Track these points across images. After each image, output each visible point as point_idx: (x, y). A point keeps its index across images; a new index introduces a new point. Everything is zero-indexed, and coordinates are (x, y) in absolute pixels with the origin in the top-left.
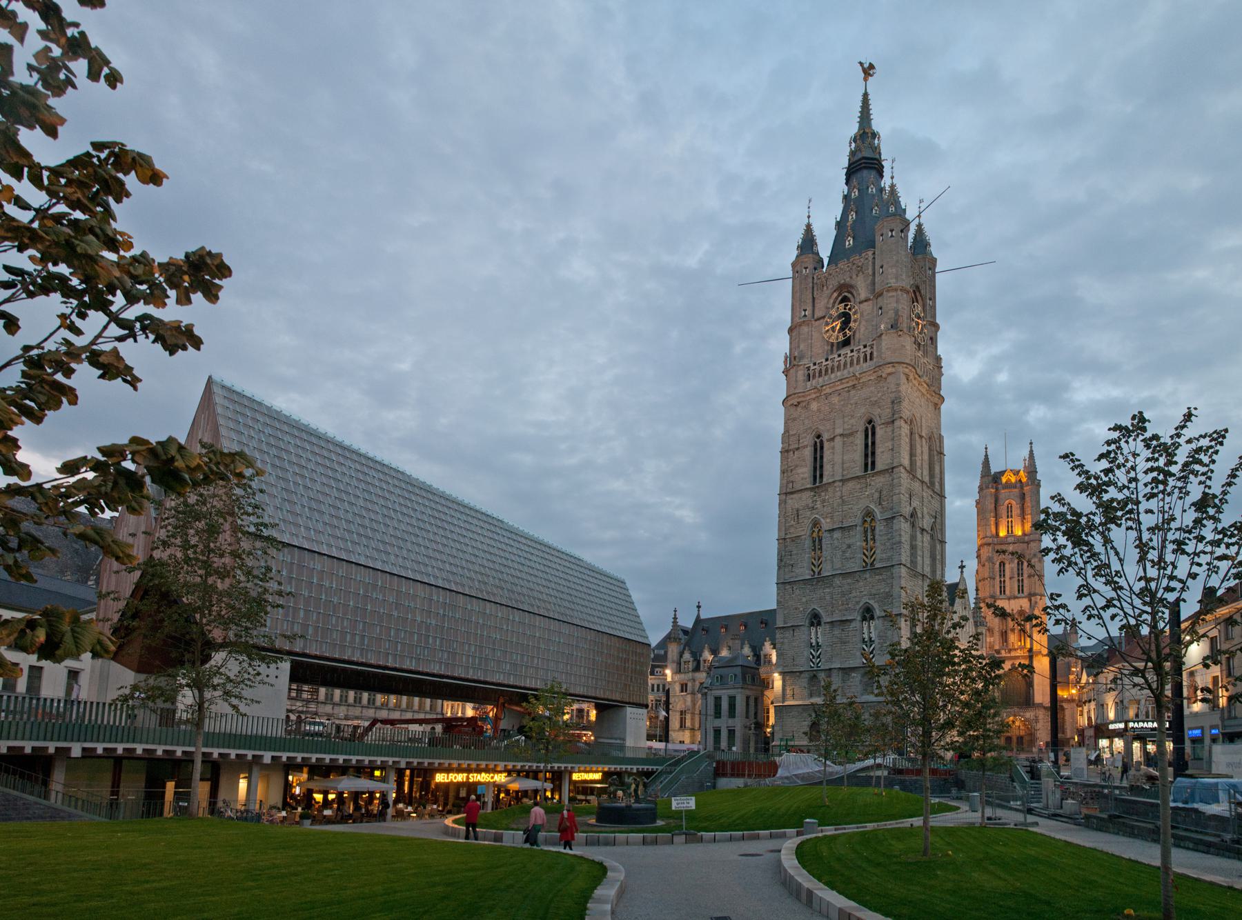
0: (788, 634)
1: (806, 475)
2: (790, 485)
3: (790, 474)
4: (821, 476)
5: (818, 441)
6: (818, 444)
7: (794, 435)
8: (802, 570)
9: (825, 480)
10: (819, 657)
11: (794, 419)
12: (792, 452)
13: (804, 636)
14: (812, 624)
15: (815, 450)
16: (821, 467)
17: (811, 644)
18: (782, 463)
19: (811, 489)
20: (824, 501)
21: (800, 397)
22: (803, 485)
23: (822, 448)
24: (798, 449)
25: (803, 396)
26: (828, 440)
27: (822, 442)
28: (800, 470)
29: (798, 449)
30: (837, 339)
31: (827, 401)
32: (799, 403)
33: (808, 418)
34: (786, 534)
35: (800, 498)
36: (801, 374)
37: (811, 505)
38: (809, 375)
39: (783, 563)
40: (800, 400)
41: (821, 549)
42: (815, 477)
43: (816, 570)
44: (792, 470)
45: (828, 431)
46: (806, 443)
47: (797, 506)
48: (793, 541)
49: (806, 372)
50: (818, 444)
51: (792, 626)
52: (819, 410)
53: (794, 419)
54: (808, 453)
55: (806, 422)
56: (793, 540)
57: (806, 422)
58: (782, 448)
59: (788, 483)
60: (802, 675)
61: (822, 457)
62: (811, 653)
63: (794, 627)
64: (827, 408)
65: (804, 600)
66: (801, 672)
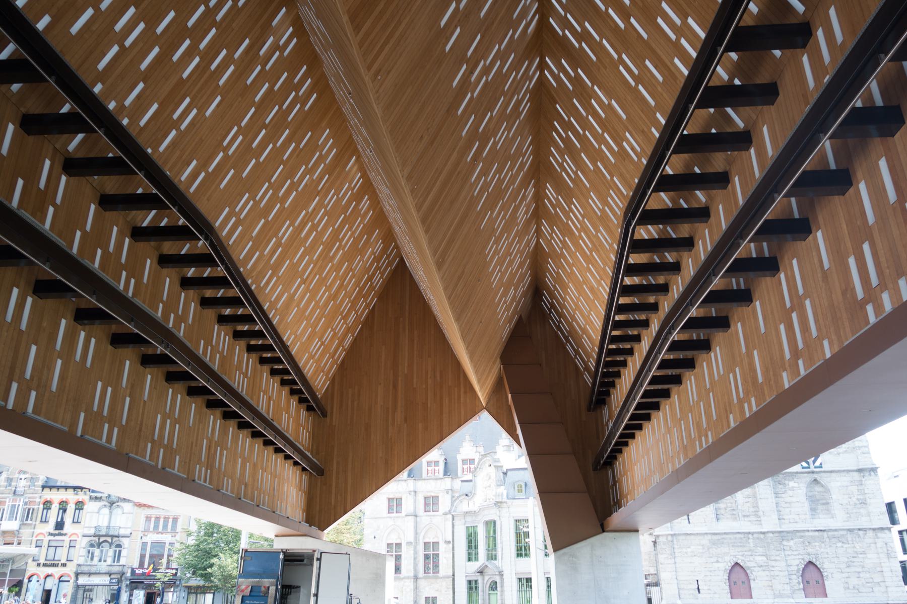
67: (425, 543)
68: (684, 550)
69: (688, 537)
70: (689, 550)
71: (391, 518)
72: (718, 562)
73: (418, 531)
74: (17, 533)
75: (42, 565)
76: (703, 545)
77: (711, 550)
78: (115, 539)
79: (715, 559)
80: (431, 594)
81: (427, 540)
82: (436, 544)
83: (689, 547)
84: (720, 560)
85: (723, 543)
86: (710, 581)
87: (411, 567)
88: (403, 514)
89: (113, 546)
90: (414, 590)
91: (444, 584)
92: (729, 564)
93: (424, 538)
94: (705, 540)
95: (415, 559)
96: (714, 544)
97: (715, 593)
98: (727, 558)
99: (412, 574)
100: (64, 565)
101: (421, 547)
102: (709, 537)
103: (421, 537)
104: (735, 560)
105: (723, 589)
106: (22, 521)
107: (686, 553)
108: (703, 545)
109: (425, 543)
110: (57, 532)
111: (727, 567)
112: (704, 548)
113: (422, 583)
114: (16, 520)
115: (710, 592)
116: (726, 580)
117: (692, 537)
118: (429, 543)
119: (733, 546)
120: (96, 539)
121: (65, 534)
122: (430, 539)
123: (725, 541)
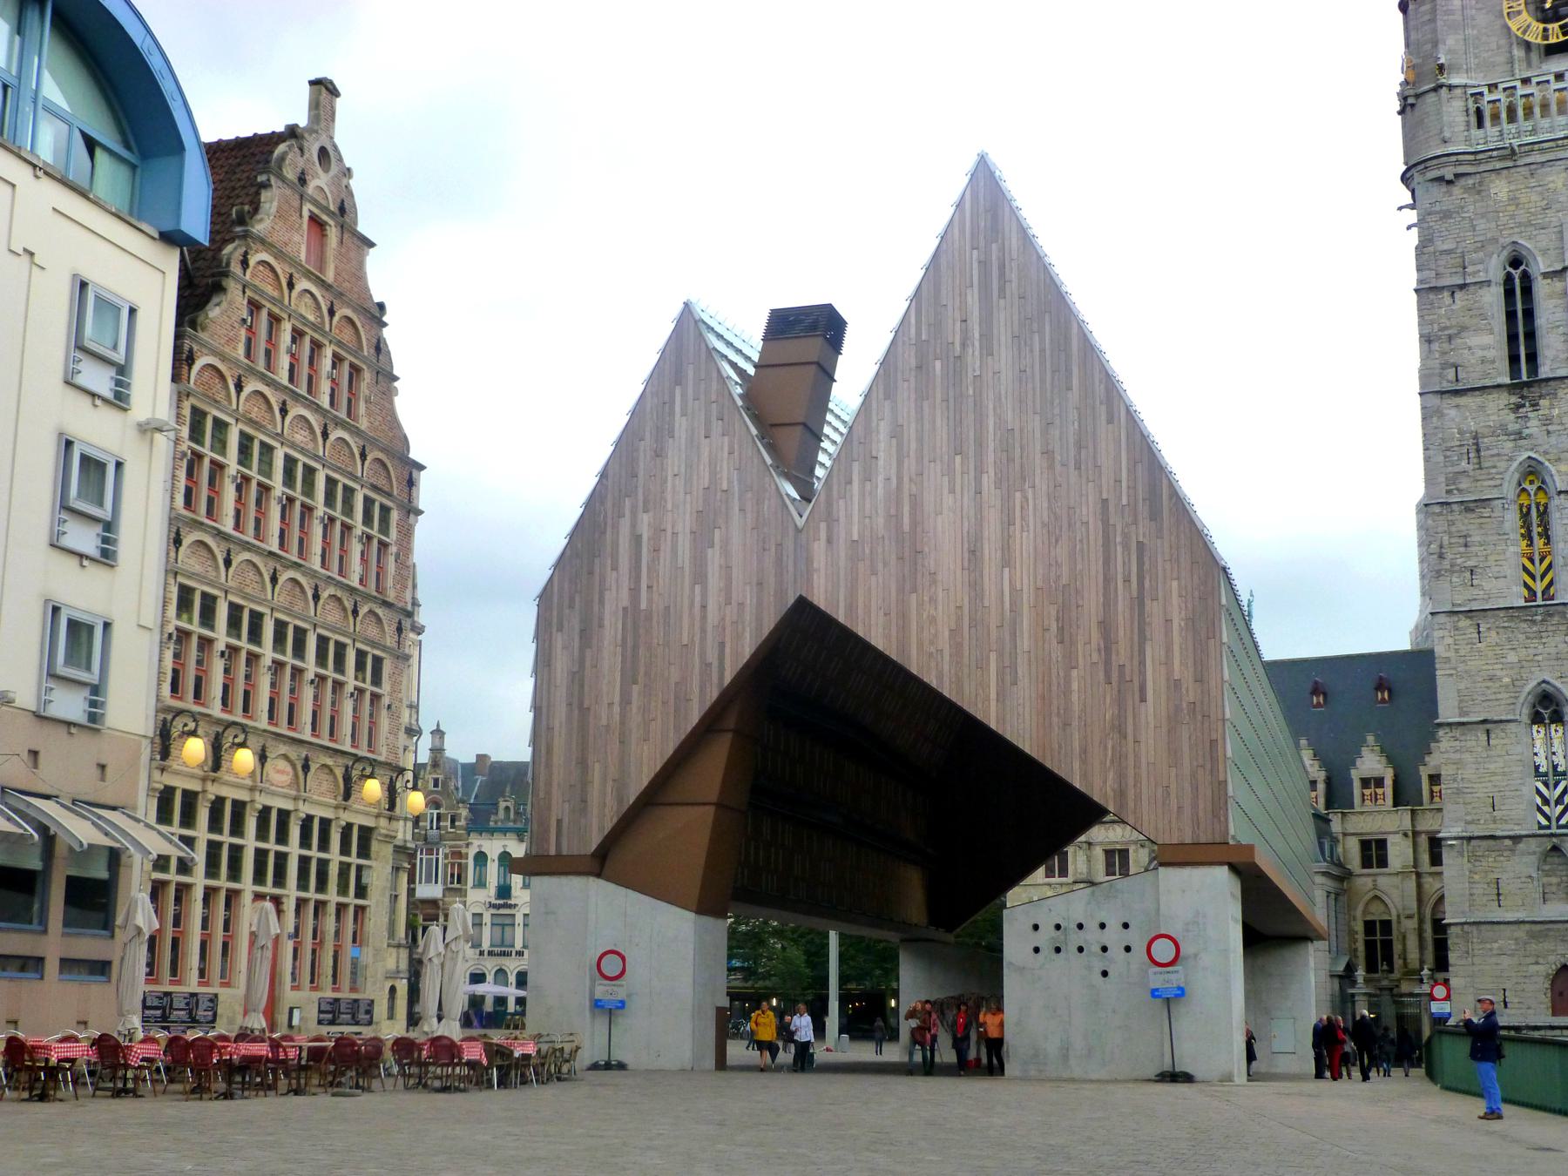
0: (1477, 739)
1: (1490, 354)
2: (1451, 374)
3: (1446, 346)
4: (1532, 358)
5: (1516, 274)
6: (1517, 282)
7: (1448, 252)
8: (1501, 583)
9: (1544, 371)
10: (1559, 801)
11: (1446, 215)
12: (1446, 294)
13: (1519, 749)
14: (1537, 719)
15: (1509, 293)
16: (1531, 336)
17: (1537, 768)
18: (1421, 317)
19: (1511, 388)
20: (1547, 421)
21: (1460, 163)
22: (1486, 375)
23: (1527, 291)
24: (1463, 287)
25: (1470, 163)
26: (1546, 275)
27: (1526, 277)
28: (1475, 340)
29: (1463, 287)
30: (1546, 38)
31: (1533, 182)
32: (1457, 176)
33: (1483, 216)
34: (1448, 492)
35: (1482, 408)
36: (1454, 111)
37: (1513, 427)
38: (1479, 113)
39: (1446, 564)
40: (1461, 170)
41: (1546, 535)
42: (1514, 359)
43: (1539, 587)
44: (1450, 338)
45: (1544, 252)
46: (1482, 277)
47: (1472, 426)
48: (1468, 510)
49: (1472, 107)
50: (1517, 282)
51: (1485, 721)
52: (1513, 200)
53: (1446, 215)
54: (1492, 299)
55: (1481, 225)
56: (1468, 507)
57: (1481, 225)
58: (1420, 281)
59: (1444, 366)
60: (1521, 846)
61: (1529, 314)
62: (1539, 792)
63: (1487, 725)
64: (1534, 198)
65: (1512, 657)
66: (1516, 839)
68: (1488, 946)
69: (1496, 927)
70: (1496, 945)
71: (1050, 885)
72: (1537, 963)
74: (441, 903)
75: (486, 953)
76: (1516, 939)
77: (1527, 946)
79: (1532, 960)
83: (1496, 942)
84: (1541, 961)
85: (1546, 936)
86: (1523, 990)
88: (1070, 879)
92: (1554, 967)
94: (1521, 932)
96: (1533, 937)
97: (1529, 1008)
98: (1552, 958)
100: (520, 954)
102: (1527, 927)
104: (1562, 960)
105: (1541, 1003)
106: (445, 883)
107: (1491, 950)
108: (1516, 939)
110: (501, 902)
111: (1550, 972)
112: (1517, 944)
114: (436, 882)
115: (1521, 1006)
116: (1547, 989)
117: (1502, 926)
119: (1562, 941)
123: (1552, 933)
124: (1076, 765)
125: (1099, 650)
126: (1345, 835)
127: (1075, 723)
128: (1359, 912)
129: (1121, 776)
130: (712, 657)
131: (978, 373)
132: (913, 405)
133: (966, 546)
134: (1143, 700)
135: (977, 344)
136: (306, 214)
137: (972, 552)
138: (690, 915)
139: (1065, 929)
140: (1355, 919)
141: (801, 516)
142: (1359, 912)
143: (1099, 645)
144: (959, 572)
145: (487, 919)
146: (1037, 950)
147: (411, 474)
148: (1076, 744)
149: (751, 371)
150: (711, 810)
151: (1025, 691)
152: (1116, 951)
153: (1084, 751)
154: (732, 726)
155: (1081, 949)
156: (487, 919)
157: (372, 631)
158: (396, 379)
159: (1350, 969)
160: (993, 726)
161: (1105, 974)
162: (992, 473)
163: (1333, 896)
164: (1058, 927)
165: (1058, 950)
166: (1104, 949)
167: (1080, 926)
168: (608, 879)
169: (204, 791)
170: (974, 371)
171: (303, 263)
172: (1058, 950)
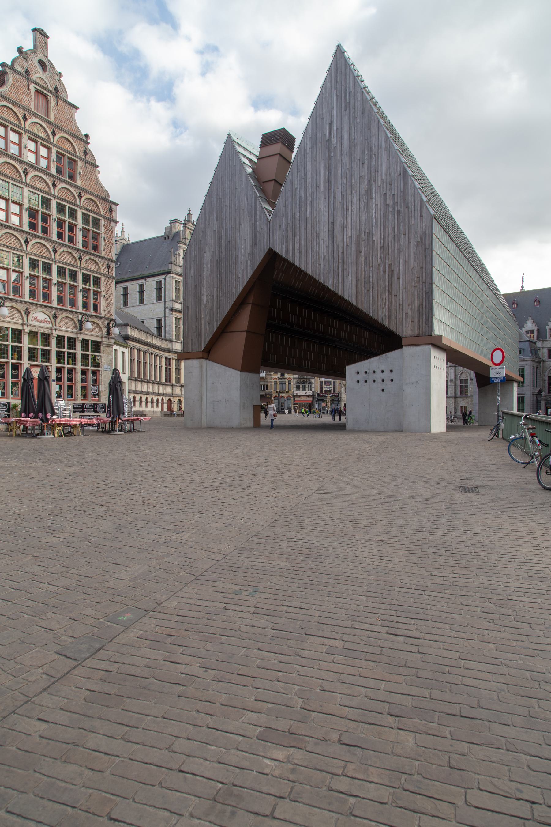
67: (461, 380)
73: (457, 374)
78: (308, 380)
80: (464, 405)
81: (462, 378)
82: (466, 381)
87: (453, 392)
89: (307, 383)
90: (454, 403)
91: (470, 400)
93: (460, 377)
95: (455, 388)
99: (453, 395)
100: (288, 392)
101: (458, 383)
103: (458, 377)
109: (461, 380)
113: (459, 400)
118: (463, 380)
120: (299, 380)
121: (286, 378)
122: (463, 377)
124: (371, 307)
125: (381, 258)
126: (542, 348)
127: (371, 290)
128: (546, 374)
129: (390, 311)
130: (240, 276)
131: (335, 145)
132: (310, 163)
133: (330, 221)
134: (398, 278)
135: (335, 133)
136: (32, 89)
137: (332, 223)
138: (239, 372)
139: (369, 373)
140: (545, 376)
141: (270, 216)
142: (546, 374)
143: (381, 256)
144: (327, 231)
145: (278, 383)
146: (358, 382)
147: (111, 207)
148: (371, 298)
149: (256, 161)
150: (245, 333)
151: (350, 279)
152: (387, 381)
153: (374, 300)
154: (251, 302)
155: (374, 381)
156: (278, 383)
157: (92, 266)
158: (98, 167)
159: (540, 392)
160: (340, 293)
161: (383, 390)
162: (340, 189)
163: (535, 368)
164: (366, 372)
165: (366, 381)
166: (383, 381)
167: (374, 372)
168: (210, 360)
169: (24, 329)
170: (334, 144)
171: (33, 110)
172: (366, 381)
